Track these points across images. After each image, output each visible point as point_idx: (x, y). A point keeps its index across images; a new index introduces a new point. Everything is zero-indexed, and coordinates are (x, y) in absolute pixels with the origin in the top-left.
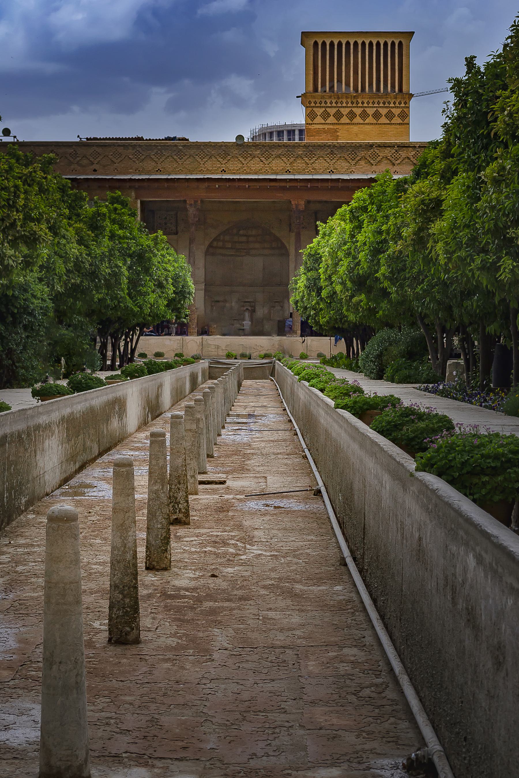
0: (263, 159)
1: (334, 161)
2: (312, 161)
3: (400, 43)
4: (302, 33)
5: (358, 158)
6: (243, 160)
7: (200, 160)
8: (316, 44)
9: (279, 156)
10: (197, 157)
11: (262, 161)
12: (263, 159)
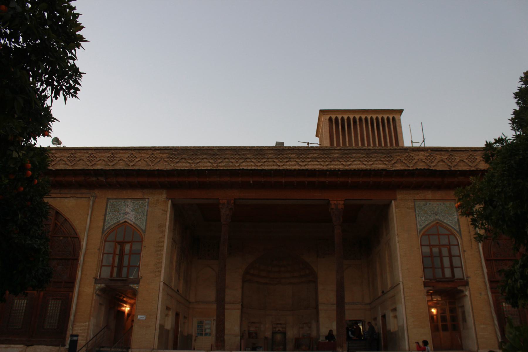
0: (299, 161)
1: (370, 163)
2: (349, 163)
3: (394, 119)
4: (321, 111)
5: (395, 160)
6: (278, 163)
7: (235, 163)
8: (330, 119)
9: (315, 159)
10: (232, 160)
11: (298, 164)
12: (299, 161)
